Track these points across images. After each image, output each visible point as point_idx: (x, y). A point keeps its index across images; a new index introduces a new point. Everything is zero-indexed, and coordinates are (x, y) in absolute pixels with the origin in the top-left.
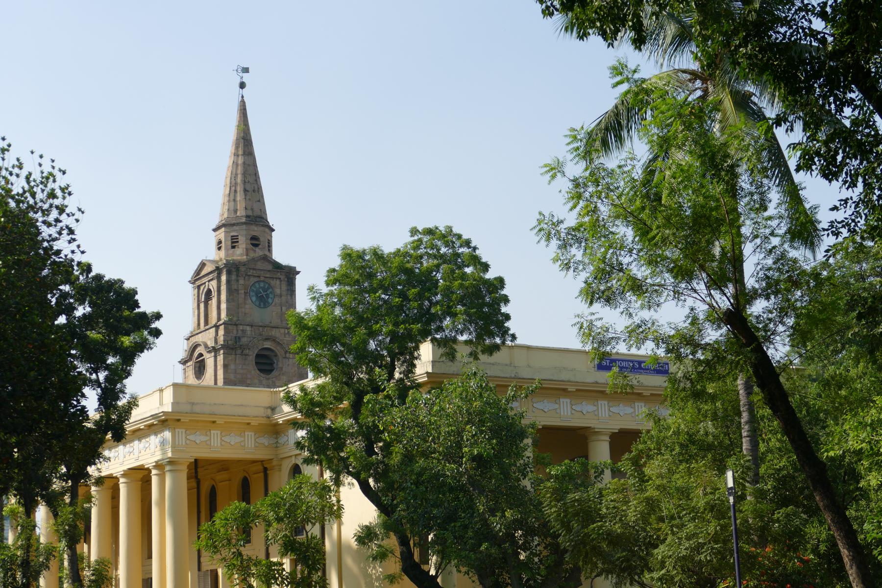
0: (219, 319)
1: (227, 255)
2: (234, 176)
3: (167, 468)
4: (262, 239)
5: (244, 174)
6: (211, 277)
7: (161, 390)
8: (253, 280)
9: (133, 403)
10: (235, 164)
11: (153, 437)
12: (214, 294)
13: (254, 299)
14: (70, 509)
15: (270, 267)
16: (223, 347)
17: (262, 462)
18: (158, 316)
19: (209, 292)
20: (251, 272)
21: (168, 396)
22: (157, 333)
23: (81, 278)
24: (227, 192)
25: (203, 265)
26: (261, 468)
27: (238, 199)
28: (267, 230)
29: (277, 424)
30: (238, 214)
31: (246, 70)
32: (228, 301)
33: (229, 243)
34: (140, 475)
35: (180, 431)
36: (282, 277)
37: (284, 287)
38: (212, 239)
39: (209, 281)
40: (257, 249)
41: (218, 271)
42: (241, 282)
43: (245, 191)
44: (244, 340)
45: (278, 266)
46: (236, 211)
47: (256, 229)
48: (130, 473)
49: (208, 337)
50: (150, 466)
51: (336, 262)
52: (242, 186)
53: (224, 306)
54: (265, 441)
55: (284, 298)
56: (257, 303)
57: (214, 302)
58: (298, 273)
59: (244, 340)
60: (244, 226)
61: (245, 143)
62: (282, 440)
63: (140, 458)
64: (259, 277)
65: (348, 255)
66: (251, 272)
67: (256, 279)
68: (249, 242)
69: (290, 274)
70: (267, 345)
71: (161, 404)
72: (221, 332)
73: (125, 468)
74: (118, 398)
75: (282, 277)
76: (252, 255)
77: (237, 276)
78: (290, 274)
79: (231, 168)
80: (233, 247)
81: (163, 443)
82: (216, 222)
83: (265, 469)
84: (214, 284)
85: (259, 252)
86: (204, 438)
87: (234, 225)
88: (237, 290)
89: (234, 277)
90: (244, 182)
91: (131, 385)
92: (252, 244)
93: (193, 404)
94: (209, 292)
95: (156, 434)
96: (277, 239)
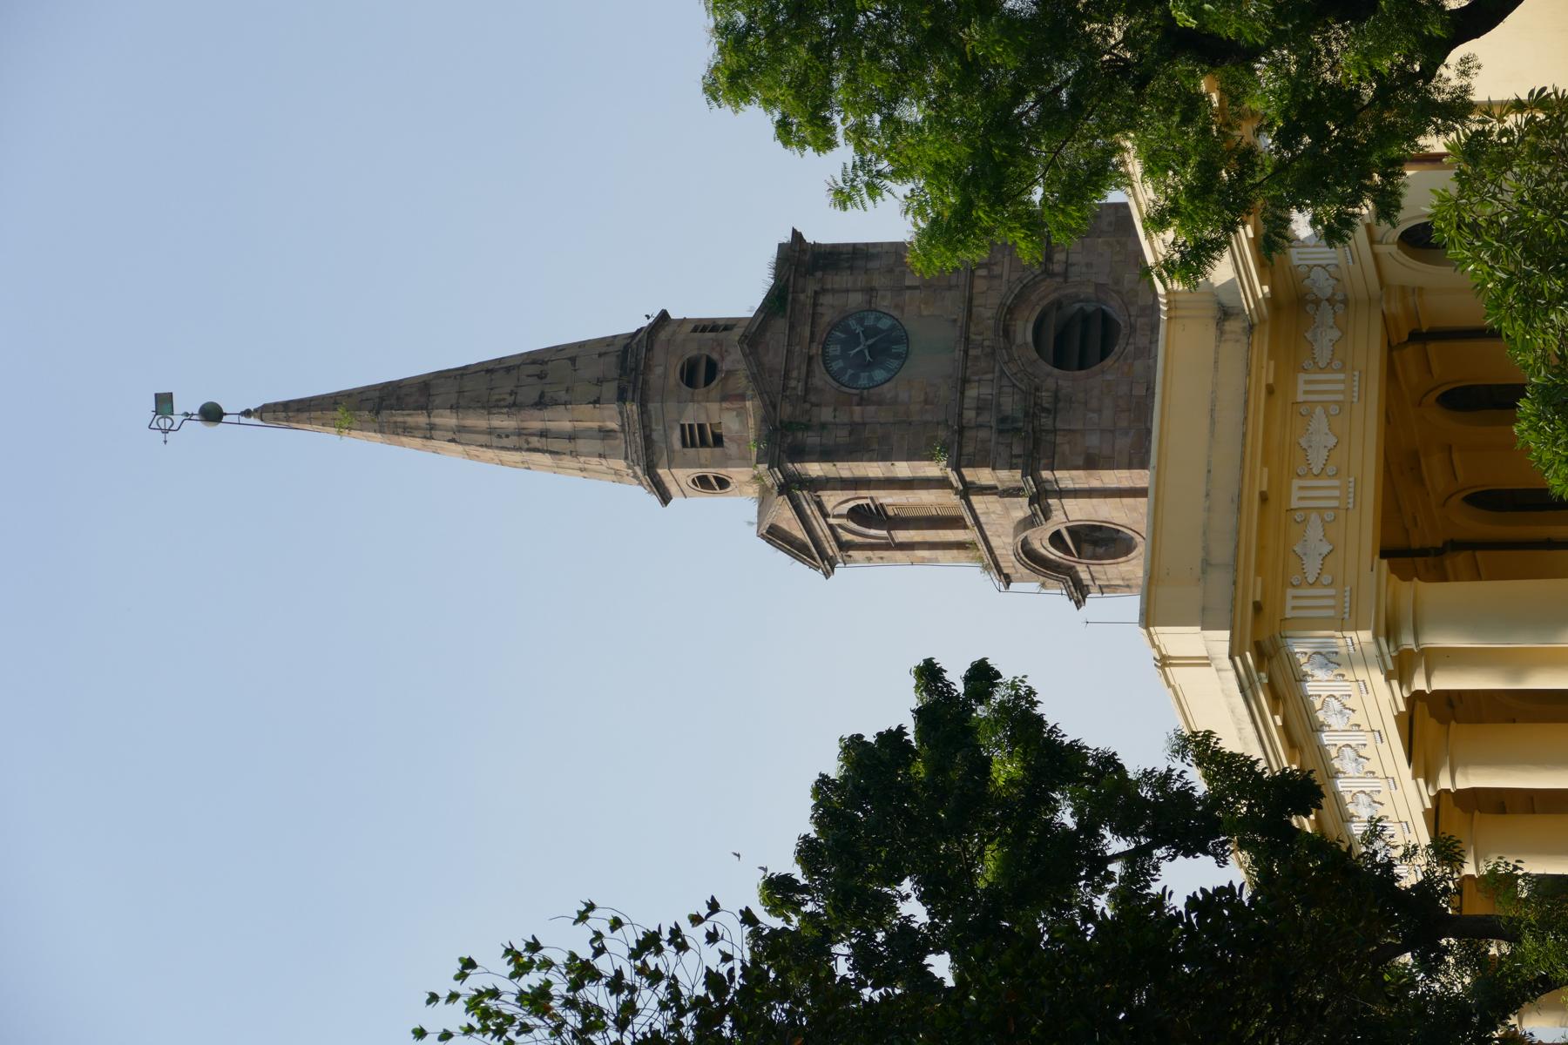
0: (942, 483)
1: (743, 461)
2: (496, 440)
3: (1408, 642)
4: (692, 352)
5: (490, 406)
6: (811, 510)
7: (1164, 662)
8: (820, 378)
9: (1201, 747)
10: (458, 436)
11: (1311, 688)
12: (865, 497)
13: (879, 375)
14: (1529, 942)
15: (781, 325)
16: (1030, 470)
17: (1391, 348)
18: (929, 674)
19: (861, 515)
20: (796, 385)
21: (1182, 639)
22: (982, 675)
23: (809, 908)
24: (546, 459)
25: (774, 535)
26: (1411, 352)
27: (566, 425)
28: (663, 336)
29: (1273, 301)
30: (613, 425)
31: (164, 403)
32: (885, 456)
33: (705, 452)
34: (1429, 727)
35: (1292, 603)
36: (812, 286)
37: (842, 280)
38: (692, 507)
39: (825, 515)
40: (725, 366)
41: (791, 487)
42: (826, 414)
43: (541, 403)
44: (1010, 404)
45: (776, 301)
46: (605, 434)
47: (659, 370)
48: (1421, 756)
49: (1001, 518)
50: (1401, 695)
51: (757, 120)
52: (526, 413)
53: (903, 469)
54: (1325, 338)
55: (878, 281)
56: (894, 364)
57: (890, 499)
58: (797, 235)
59: (1010, 404)
60: (651, 406)
61: (391, 407)
62: (1322, 284)
63: (1377, 726)
64: (810, 358)
65: (735, 79)
66: (796, 385)
67: (818, 368)
68: (702, 390)
69: (801, 263)
70: (1024, 332)
71: (1205, 661)
72: (984, 476)
73: (1406, 771)
74: (1186, 794)
75: (812, 286)
77: (807, 427)
78: (801, 263)
79: (472, 449)
80: (718, 440)
81: (1330, 660)
82: (639, 496)
83: (1415, 338)
84: (831, 499)
85: (734, 360)
86: (1315, 531)
87: (648, 441)
88: (854, 428)
89: (812, 439)
90: (515, 406)
91: (1143, 752)
92: (708, 382)
93: (1206, 564)
94: (861, 515)
95: (1301, 678)
96: (687, 307)
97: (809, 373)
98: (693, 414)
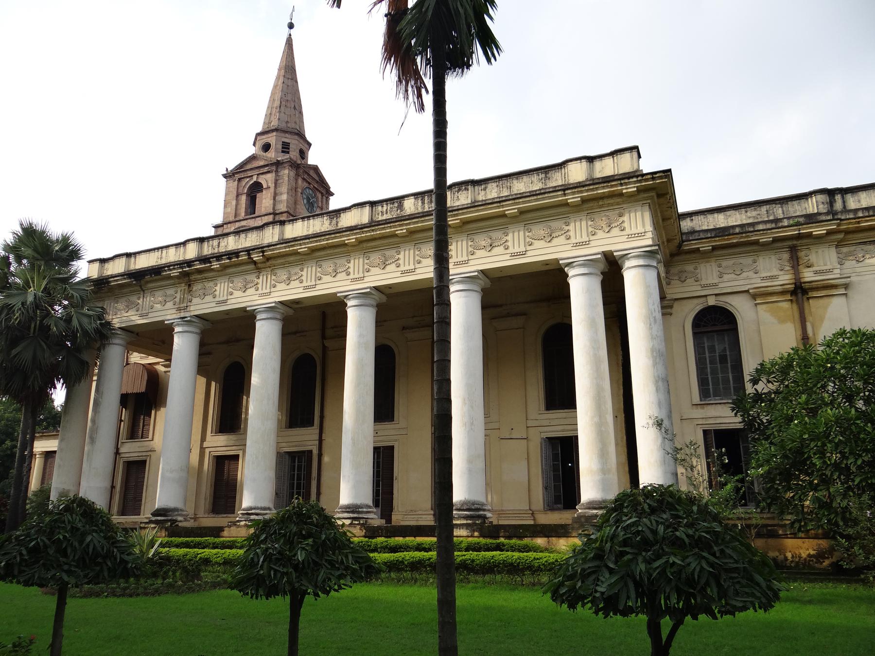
0: (274, 208)
6: (266, 169)
33: (280, 147)
53: (284, 197)
58: (332, 194)
60: (296, 137)
64: (309, 183)
76: (299, 162)
77: (297, 175)
80: (283, 152)
82: (259, 129)
97: (307, 182)
98: (291, 146)
